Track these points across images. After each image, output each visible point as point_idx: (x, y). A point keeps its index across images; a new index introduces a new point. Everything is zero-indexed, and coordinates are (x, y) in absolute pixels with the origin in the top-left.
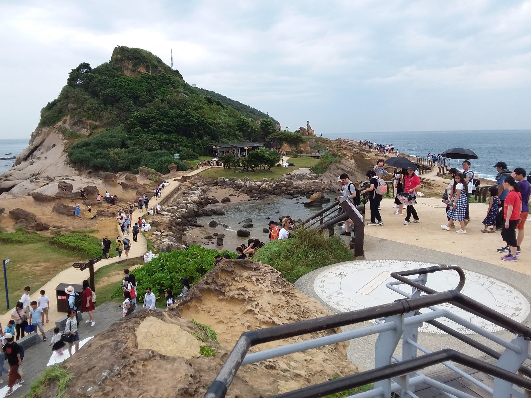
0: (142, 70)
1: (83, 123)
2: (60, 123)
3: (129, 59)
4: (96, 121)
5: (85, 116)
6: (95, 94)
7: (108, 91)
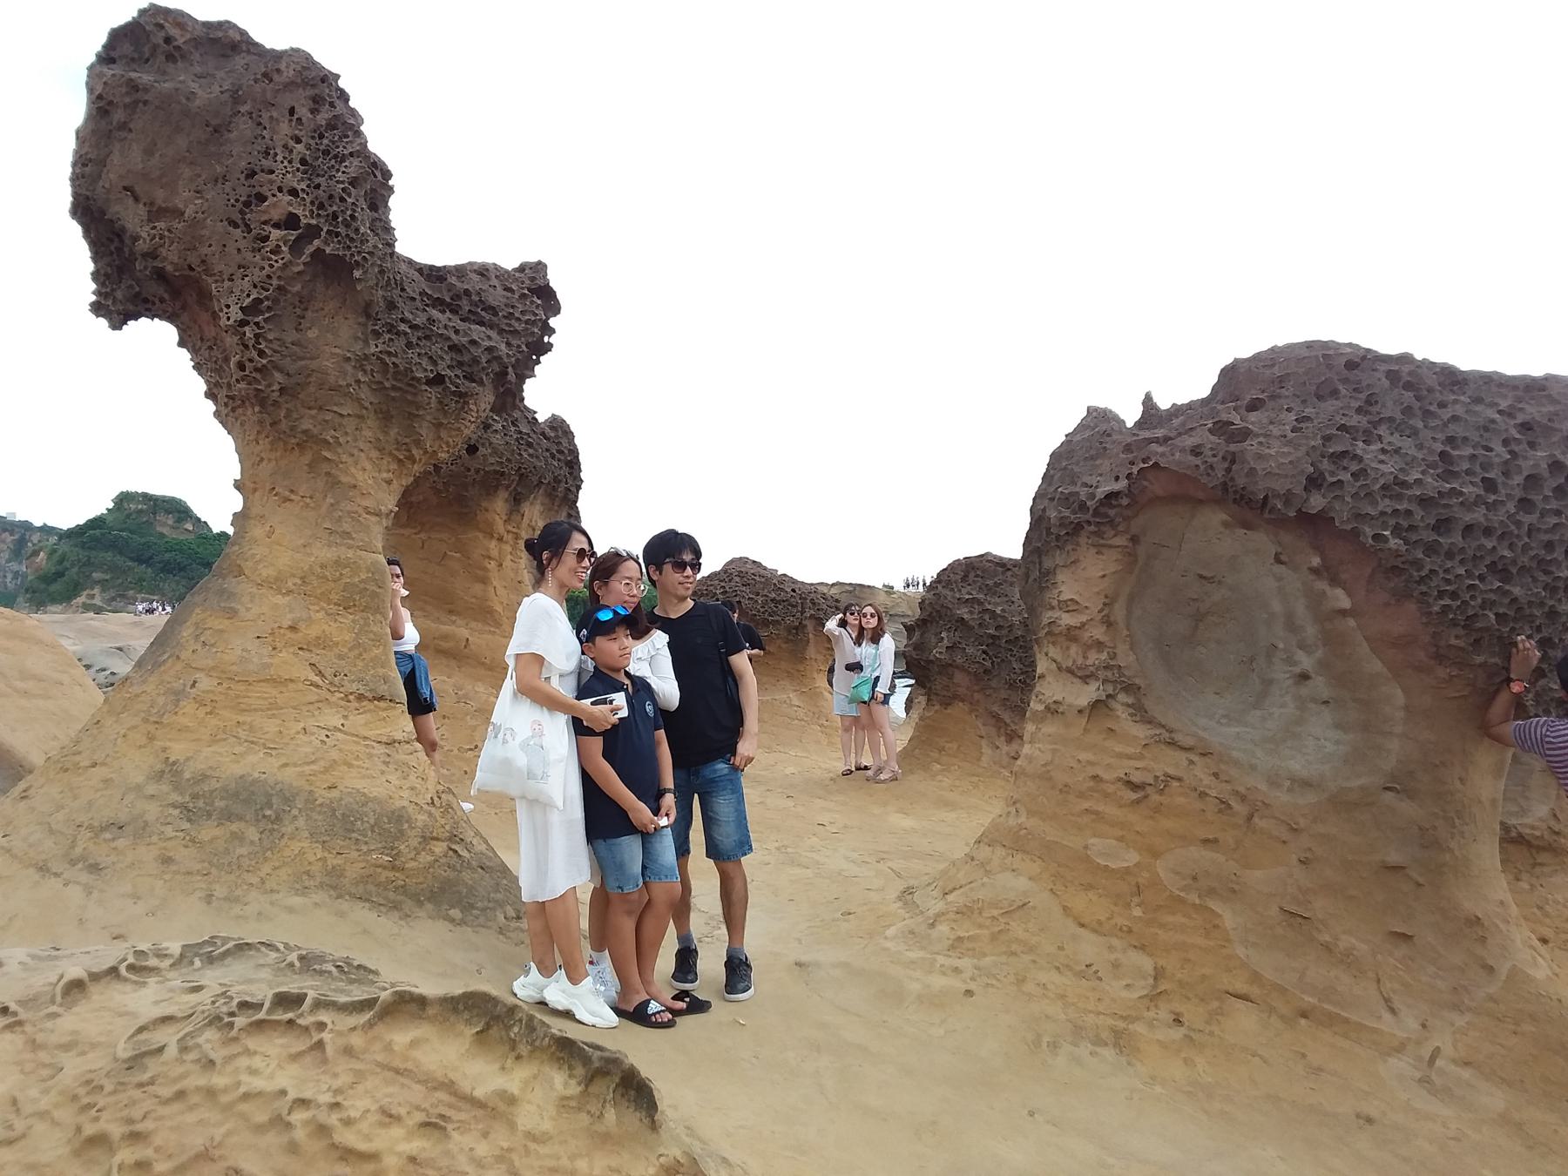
1: (128, 599)
2: (81, 600)
3: (168, 512)
4: (153, 594)
5: (132, 589)
6: (140, 560)
7: (167, 556)
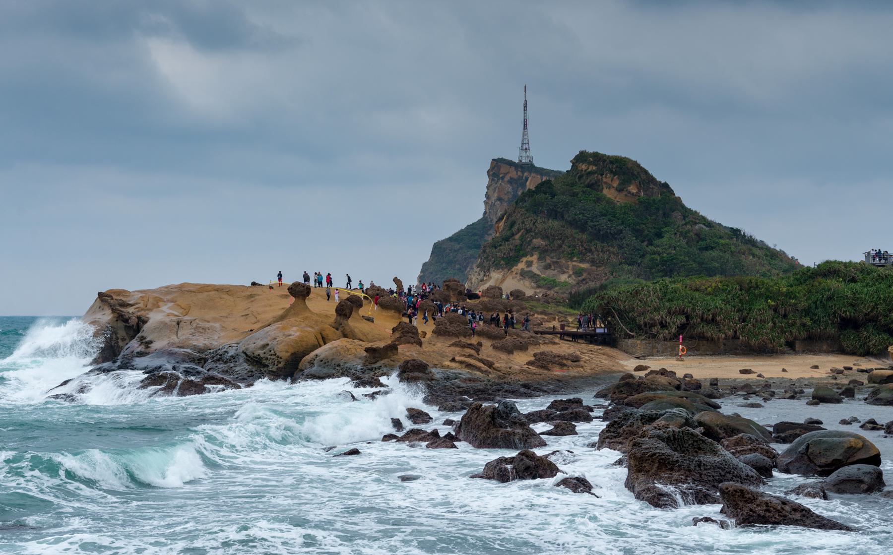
0: (633, 189)
2: (521, 266)
